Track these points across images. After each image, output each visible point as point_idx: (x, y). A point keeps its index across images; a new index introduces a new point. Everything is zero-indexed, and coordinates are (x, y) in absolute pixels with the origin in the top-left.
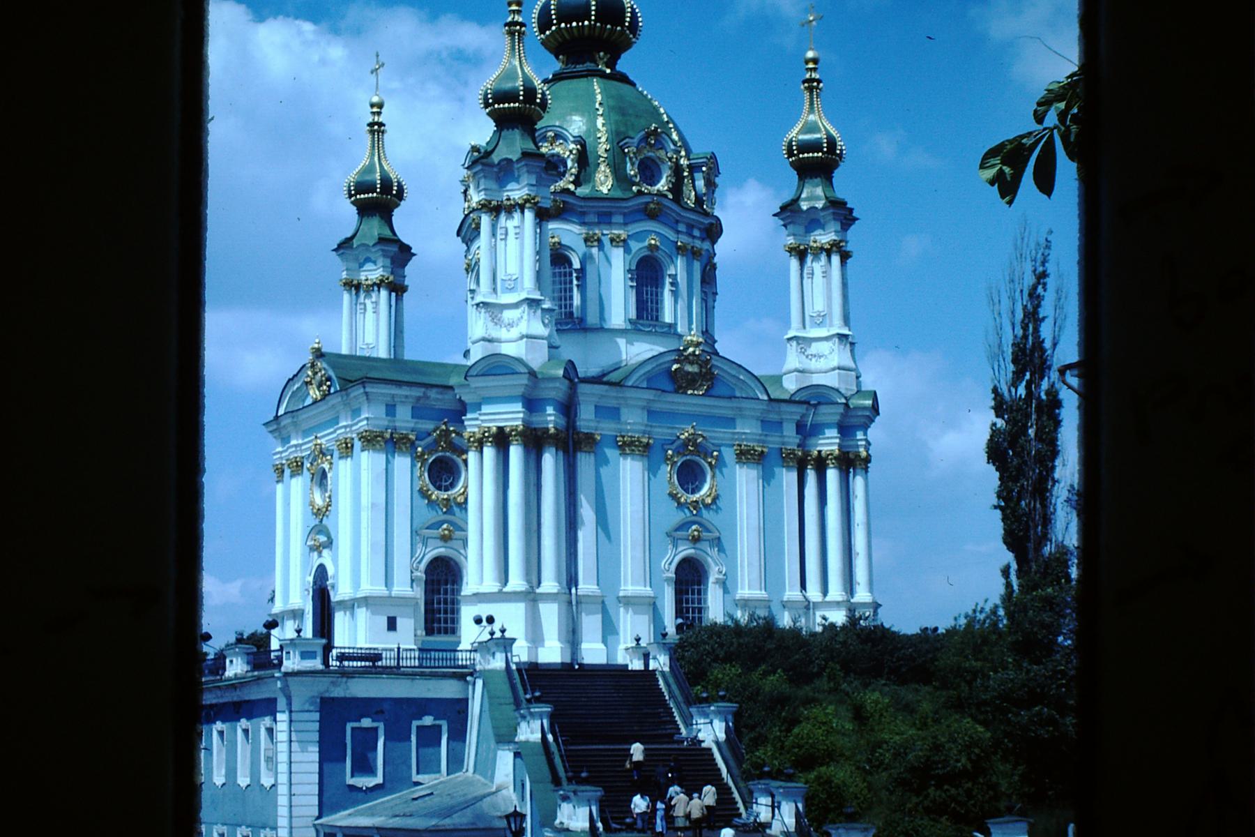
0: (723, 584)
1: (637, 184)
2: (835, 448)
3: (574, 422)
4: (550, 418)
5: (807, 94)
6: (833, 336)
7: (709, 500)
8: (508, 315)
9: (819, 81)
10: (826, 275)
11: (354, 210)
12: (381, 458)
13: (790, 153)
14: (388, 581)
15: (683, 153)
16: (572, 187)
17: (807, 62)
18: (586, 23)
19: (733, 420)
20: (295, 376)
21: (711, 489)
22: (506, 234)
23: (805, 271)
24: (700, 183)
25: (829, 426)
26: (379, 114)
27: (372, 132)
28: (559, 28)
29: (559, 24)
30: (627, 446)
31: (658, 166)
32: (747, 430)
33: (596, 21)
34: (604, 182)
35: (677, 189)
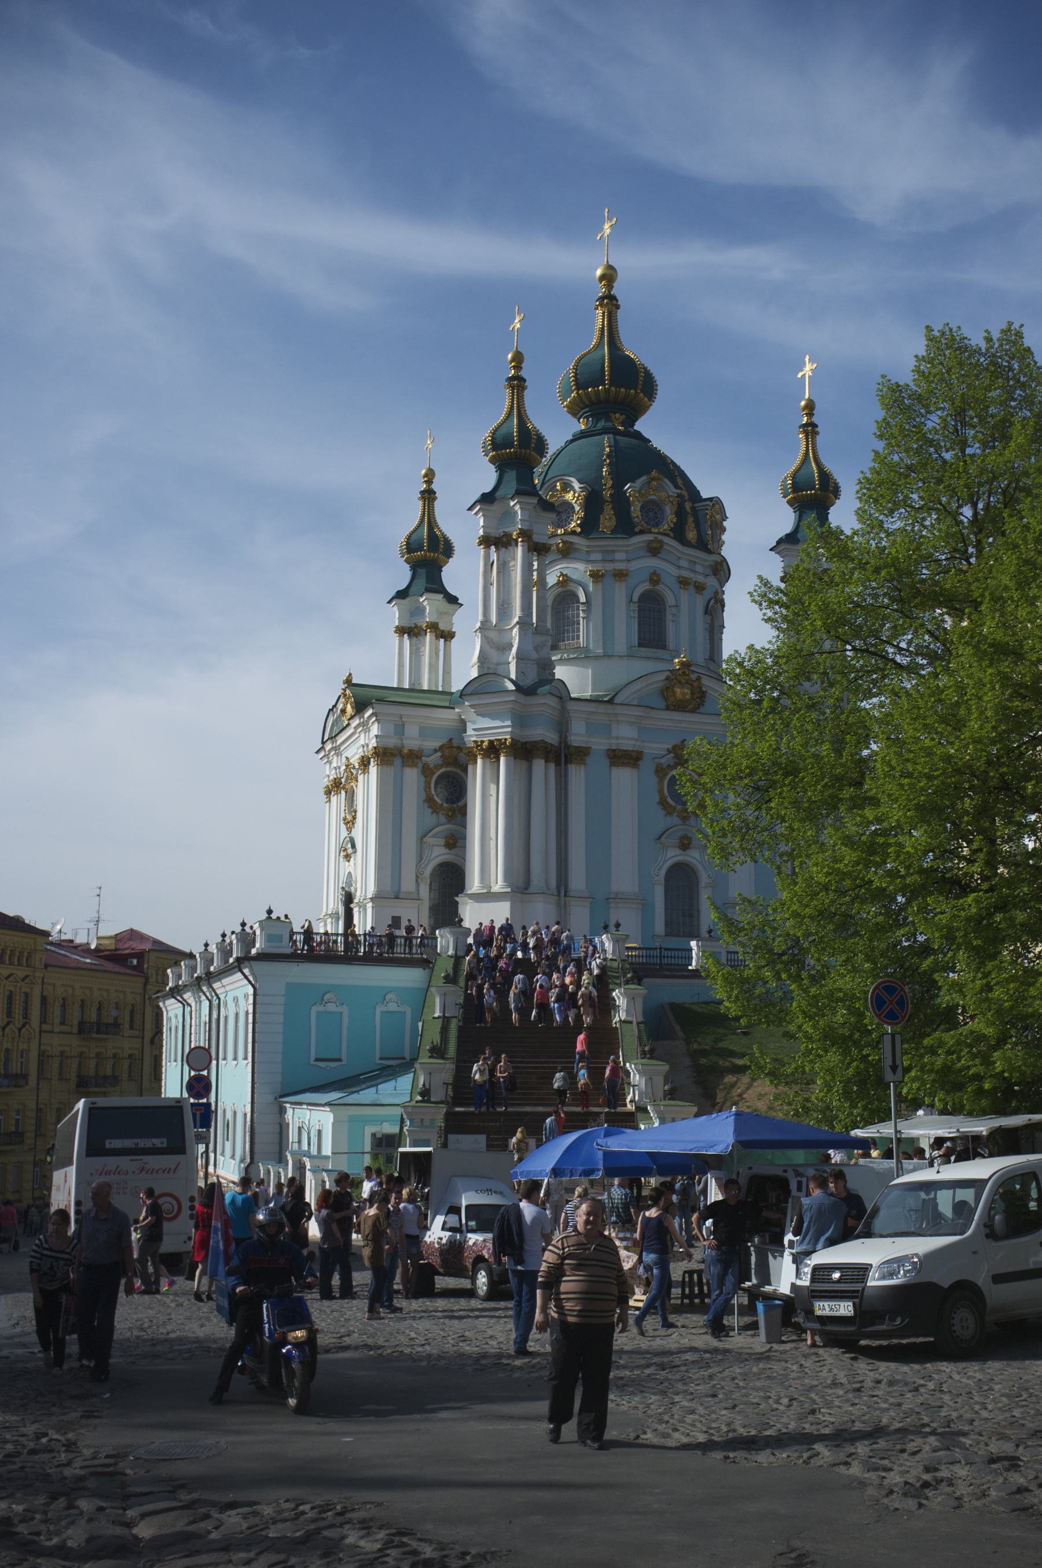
3: (566, 737)
11: (407, 567)
12: (390, 770)
15: (687, 498)
20: (335, 706)
26: (429, 482)
27: (423, 498)
29: (578, 389)
33: (611, 385)
34: (607, 520)
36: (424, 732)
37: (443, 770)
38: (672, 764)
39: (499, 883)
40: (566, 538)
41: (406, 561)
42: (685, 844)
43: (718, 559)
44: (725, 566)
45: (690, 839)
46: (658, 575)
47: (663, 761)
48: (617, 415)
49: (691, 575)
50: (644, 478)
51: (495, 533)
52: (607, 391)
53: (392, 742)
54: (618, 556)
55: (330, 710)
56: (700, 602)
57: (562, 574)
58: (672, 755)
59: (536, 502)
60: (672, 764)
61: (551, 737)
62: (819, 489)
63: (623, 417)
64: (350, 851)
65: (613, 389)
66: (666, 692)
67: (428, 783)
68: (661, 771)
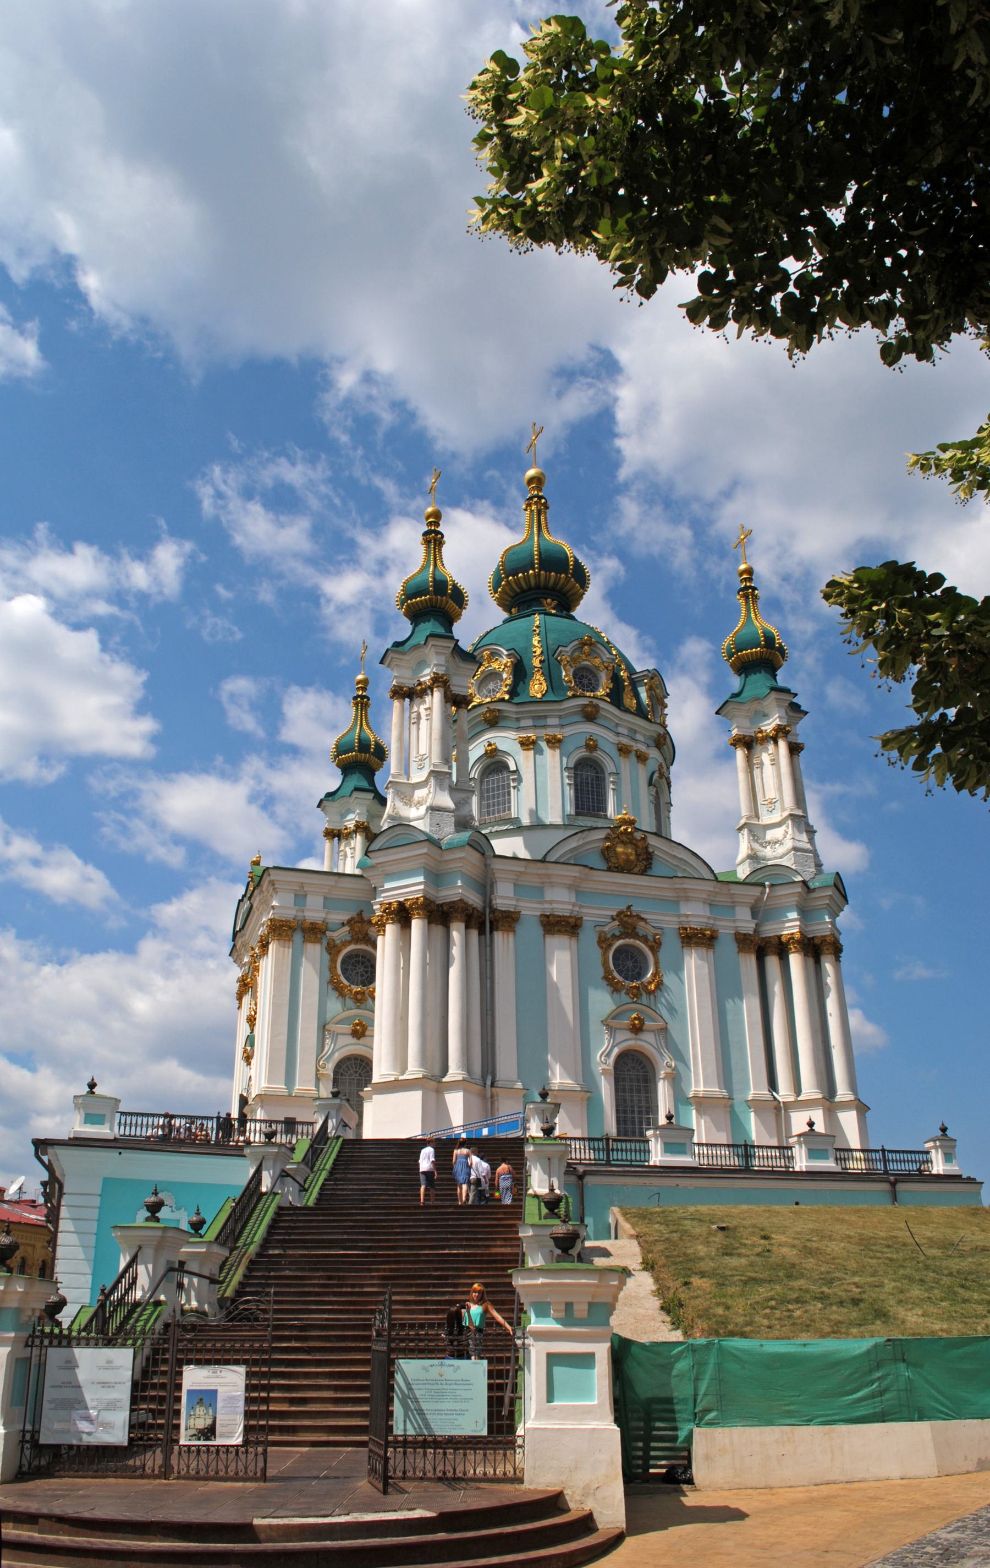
1: (570, 689)
2: (796, 930)
3: (491, 901)
4: (457, 890)
5: (742, 601)
6: (786, 818)
7: (653, 987)
8: (419, 794)
10: (775, 762)
11: (339, 771)
14: (290, 1079)
16: (507, 697)
18: (531, 572)
20: (244, 896)
21: (654, 975)
24: (644, 695)
26: (364, 689)
27: (356, 705)
28: (508, 582)
31: (595, 676)
32: (695, 914)
33: (540, 570)
36: (328, 902)
37: (352, 947)
39: (410, 1068)
40: (492, 707)
41: (338, 766)
42: (637, 1029)
43: (661, 731)
44: (668, 739)
45: (642, 1021)
46: (594, 741)
47: (606, 929)
48: (549, 600)
50: (577, 642)
51: (409, 683)
52: (537, 576)
53: (290, 913)
54: (550, 721)
55: (240, 901)
56: (643, 774)
57: (490, 745)
58: (617, 923)
59: (452, 646)
60: (617, 934)
61: (474, 899)
62: (765, 646)
63: (555, 602)
64: (249, 1048)
66: (606, 853)
67: (333, 961)
68: (604, 942)
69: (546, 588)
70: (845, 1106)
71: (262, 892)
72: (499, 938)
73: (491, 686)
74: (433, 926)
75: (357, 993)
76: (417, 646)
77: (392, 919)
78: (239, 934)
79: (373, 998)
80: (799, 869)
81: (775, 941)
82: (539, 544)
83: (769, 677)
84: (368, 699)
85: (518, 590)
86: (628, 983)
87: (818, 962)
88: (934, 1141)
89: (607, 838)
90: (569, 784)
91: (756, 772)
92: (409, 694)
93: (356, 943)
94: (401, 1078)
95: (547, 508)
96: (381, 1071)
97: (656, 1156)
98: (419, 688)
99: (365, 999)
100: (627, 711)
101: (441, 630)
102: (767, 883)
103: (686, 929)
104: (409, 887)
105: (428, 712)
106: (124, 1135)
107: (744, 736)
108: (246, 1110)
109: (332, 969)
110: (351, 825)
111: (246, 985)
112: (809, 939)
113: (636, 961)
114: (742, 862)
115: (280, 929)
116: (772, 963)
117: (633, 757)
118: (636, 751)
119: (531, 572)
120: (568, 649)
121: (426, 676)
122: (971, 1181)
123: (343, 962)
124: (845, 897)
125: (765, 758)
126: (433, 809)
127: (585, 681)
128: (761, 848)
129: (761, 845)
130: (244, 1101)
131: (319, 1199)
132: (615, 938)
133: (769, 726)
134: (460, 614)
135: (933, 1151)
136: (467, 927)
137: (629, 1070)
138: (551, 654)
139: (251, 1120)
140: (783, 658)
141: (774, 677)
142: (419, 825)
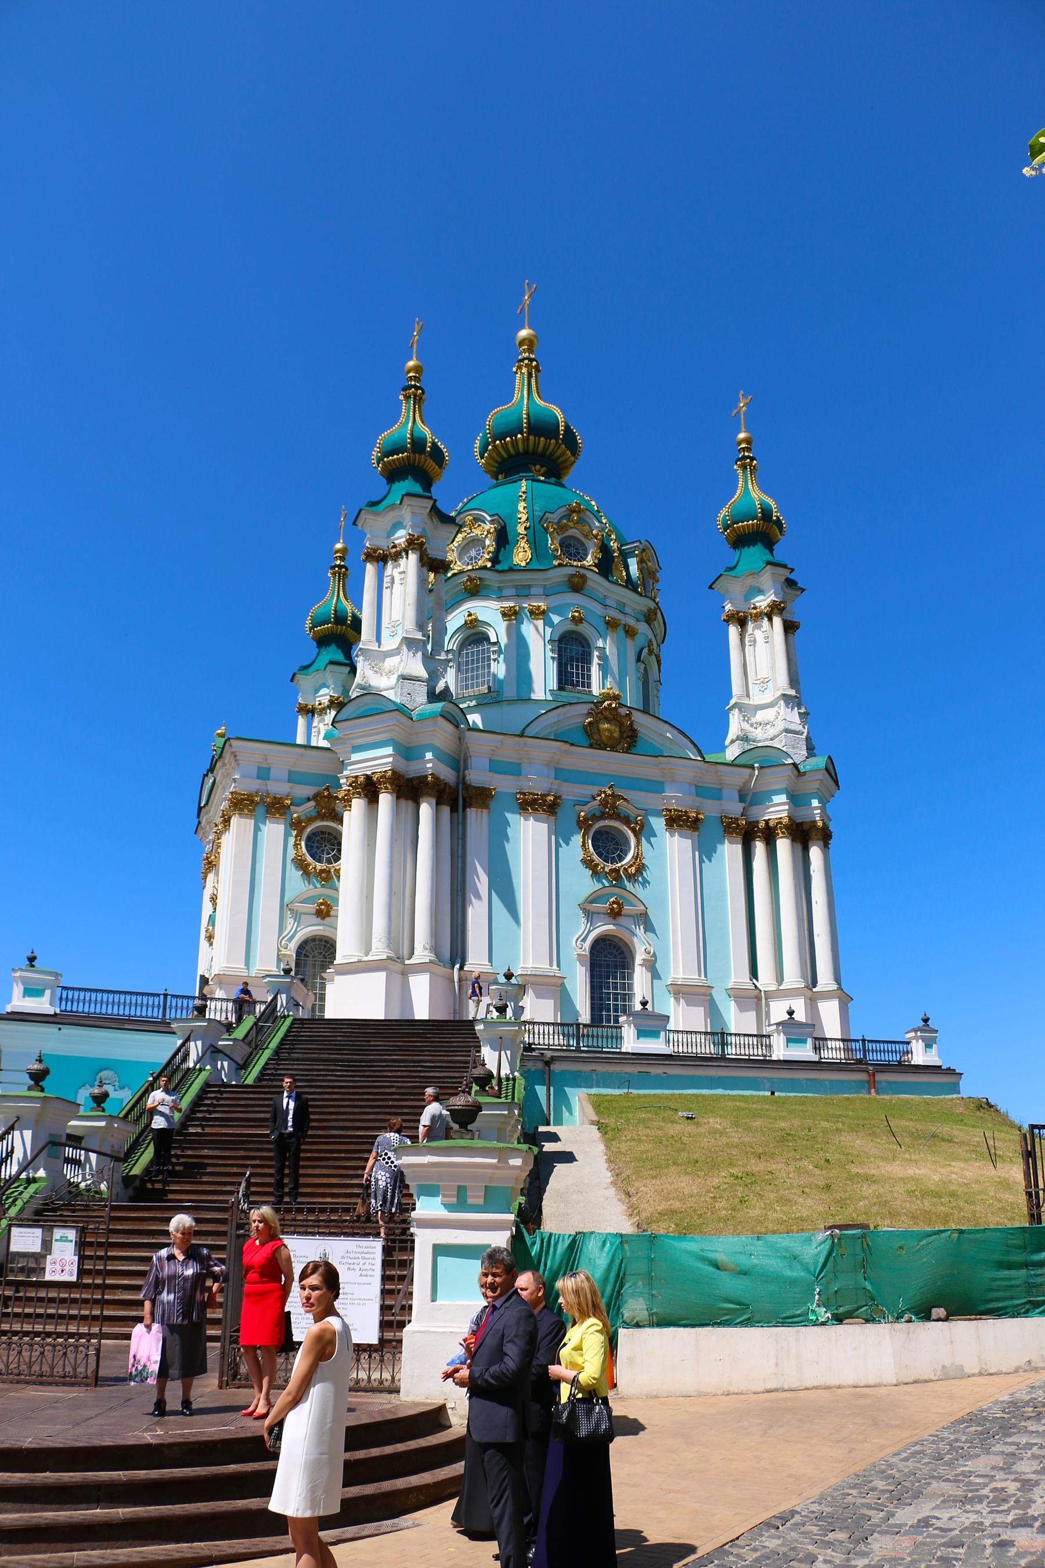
0: (651, 965)
1: (556, 558)
3: (464, 777)
4: (429, 763)
5: (740, 471)
7: (633, 870)
8: (390, 662)
9: (752, 459)
13: (726, 527)
16: (489, 565)
17: (740, 443)
18: (519, 436)
19: (662, 783)
20: (208, 771)
21: (636, 857)
22: (393, 582)
23: (747, 639)
25: (777, 792)
27: (334, 574)
28: (495, 447)
30: (529, 804)
33: (529, 434)
35: (606, 565)
38: (598, 814)
40: (473, 575)
47: (586, 808)
48: (538, 467)
49: (620, 617)
51: (383, 544)
52: (525, 440)
57: (470, 615)
60: (598, 814)
61: (447, 774)
64: (210, 928)
65: (531, 437)
69: (534, 453)
70: (826, 995)
71: (224, 764)
72: (472, 813)
73: (473, 553)
74: (403, 802)
75: (322, 871)
76: (392, 507)
77: (359, 793)
78: (203, 810)
79: (339, 877)
80: (790, 751)
81: (762, 825)
82: (528, 408)
83: (767, 551)
84: (347, 569)
85: (505, 455)
86: (609, 867)
87: (806, 849)
88: (915, 1031)
89: (589, 714)
90: (553, 658)
91: (748, 649)
92: (382, 558)
93: (322, 819)
94: (364, 959)
95: (537, 368)
96: (346, 951)
97: (629, 1043)
98: (394, 550)
99: (328, 878)
100: (616, 583)
101: (418, 489)
102: (756, 765)
103: (670, 811)
104: (377, 760)
105: (403, 576)
106: (66, 1011)
107: (738, 612)
108: (205, 991)
109: (296, 845)
110: (325, 701)
111: (210, 863)
112: (798, 825)
113: (617, 843)
114: (732, 742)
115: (242, 804)
116: (759, 848)
117: (621, 631)
118: (625, 625)
119: (519, 436)
120: (554, 516)
121: (401, 537)
122: (950, 1072)
123: (309, 839)
124: (836, 782)
125: (759, 635)
126: (404, 678)
127: (573, 551)
128: (752, 729)
129: (752, 725)
130: (204, 981)
131: (259, 1079)
132: (595, 818)
133: (763, 602)
134: (440, 474)
135: (914, 1041)
136: (438, 804)
137: (605, 956)
138: (537, 520)
139: (211, 999)
140: (781, 532)
141: (771, 551)
142: (390, 695)
